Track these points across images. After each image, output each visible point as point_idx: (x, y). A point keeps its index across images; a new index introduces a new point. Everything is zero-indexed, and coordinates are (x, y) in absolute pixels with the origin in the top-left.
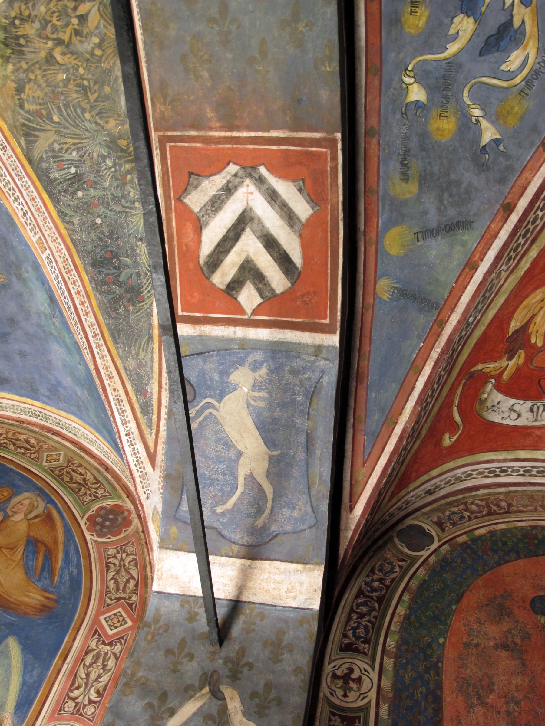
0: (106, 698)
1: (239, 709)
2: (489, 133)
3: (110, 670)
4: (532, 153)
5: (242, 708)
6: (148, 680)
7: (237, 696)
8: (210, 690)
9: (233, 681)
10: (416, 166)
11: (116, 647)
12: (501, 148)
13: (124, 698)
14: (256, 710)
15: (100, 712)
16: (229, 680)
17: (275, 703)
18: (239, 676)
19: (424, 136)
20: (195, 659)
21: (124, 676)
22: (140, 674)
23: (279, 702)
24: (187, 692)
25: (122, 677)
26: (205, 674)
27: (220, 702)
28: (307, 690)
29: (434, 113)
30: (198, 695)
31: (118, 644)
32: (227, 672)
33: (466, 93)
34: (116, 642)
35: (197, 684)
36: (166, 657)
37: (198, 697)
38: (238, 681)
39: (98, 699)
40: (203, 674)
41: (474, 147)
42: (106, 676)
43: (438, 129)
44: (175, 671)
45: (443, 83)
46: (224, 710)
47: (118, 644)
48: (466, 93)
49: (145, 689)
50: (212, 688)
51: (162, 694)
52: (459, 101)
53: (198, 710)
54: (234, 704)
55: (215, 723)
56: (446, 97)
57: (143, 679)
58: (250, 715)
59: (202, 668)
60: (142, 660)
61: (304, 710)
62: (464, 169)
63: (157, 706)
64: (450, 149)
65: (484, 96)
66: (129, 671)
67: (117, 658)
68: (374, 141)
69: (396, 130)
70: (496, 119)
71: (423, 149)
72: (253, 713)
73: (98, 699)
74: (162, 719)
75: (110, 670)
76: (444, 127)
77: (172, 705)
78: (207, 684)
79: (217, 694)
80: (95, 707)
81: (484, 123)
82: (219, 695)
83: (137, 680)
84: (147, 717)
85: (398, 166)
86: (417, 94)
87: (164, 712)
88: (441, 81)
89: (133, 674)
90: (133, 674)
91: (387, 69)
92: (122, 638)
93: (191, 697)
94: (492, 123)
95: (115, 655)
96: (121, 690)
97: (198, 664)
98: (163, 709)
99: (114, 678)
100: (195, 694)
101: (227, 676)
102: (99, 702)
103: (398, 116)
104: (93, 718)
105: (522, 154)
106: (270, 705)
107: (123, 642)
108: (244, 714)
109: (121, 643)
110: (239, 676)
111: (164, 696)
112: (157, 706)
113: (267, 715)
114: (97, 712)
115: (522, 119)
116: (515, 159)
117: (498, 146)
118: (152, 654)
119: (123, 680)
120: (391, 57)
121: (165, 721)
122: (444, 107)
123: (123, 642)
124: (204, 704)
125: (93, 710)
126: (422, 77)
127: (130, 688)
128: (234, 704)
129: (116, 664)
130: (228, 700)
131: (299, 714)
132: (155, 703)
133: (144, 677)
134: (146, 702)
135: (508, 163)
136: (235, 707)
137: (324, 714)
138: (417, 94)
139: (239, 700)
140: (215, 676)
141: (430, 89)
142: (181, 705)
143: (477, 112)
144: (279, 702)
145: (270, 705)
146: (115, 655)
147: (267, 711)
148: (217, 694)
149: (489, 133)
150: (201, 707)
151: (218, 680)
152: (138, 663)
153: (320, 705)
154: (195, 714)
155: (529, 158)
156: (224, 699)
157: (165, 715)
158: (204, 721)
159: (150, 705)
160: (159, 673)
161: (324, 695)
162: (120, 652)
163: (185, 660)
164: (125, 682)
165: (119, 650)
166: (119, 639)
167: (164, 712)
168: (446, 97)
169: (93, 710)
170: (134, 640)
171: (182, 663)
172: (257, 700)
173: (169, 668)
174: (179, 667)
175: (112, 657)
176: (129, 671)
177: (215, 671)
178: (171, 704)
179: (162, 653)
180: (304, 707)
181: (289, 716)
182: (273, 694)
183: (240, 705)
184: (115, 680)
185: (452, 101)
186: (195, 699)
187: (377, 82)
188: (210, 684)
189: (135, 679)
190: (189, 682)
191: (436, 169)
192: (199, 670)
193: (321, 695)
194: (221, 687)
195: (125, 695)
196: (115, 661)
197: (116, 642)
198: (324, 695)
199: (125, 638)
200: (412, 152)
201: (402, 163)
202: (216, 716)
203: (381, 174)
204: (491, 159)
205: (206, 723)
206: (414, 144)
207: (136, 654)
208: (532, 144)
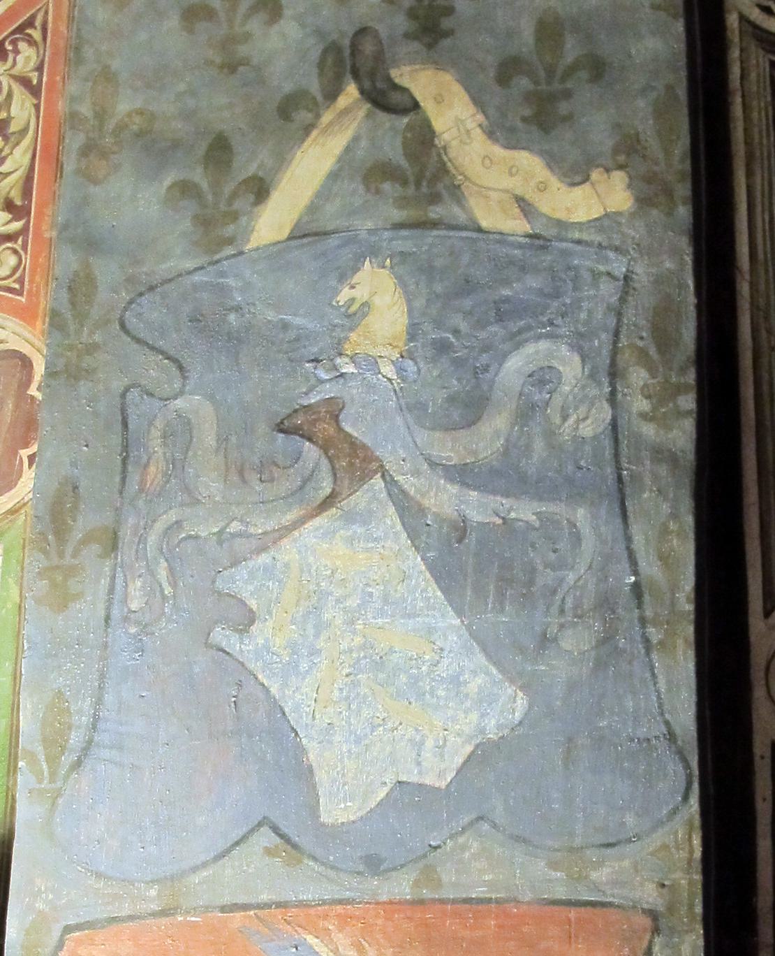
0: (40, 214)
1: (471, 124)
3: (24, 131)
5: (480, 117)
6: (153, 117)
7: (457, 88)
8: (362, 92)
9: (430, 46)
11: (19, 58)
13: (93, 190)
14: (527, 112)
15: (35, 257)
16: (415, 46)
17: (584, 75)
18: (446, 23)
20: (288, 12)
21: (72, 127)
22: (123, 106)
23: (597, 68)
24: (292, 115)
25: (68, 134)
26: (332, 49)
27: (406, 120)
28: (681, 10)
30: (327, 117)
31: (22, 46)
32: (401, 23)
34: (14, 42)
35: (314, 87)
36: (191, 31)
37: (331, 124)
38: (446, 42)
39: (17, 225)
40: (325, 51)
42: (18, 152)
44: (231, 67)
46: (423, 140)
47: (22, 46)
49: (153, 147)
50: (367, 84)
51: (211, 148)
53: (340, 160)
54: (452, 112)
55: (405, 183)
57: (137, 119)
58: (512, 130)
59: (319, 33)
60: (115, 64)
61: (683, 74)
63: (204, 185)
66: (85, 109)
67: (35, 91)
72: (520, 124)
73: (17, 225)
74: (234, 217)
75: (24, 131)
77: (252, 169)
78: (349, 76)
79: (386, 98)
80: (15, 252)
82: (395, 98)
83: (121, 128)
84: (187, 225)
87: (234, 195)
89: (101, 115)
90: (101, 115)
92: (30, 23)
93: (308, 129)
95: (25, 82)
96: (78, 171)
97: (303, 26)
98: (228, 189)
99: (46, 148)
100: (318, 116)
101: (407, 36)
102: (24, 231)
104: (21, 281)
106: (569, 85)
107: (36, 34)
108: (491, 134)
109: (31, 42)
110: (446, 23)
111: (219, 151)
112: (204, 185)
113: (568, 118)
114: (27, 261)
118: (143, 36)
119: (74, 142)
121: (244, 220)
123: (36, 34)
124: (356, 139)
125: (13, 261)
127: (104, 155)
128: (452, 112)
129: (37, 107)
130: (428, 105)
131: (669, 88)
132: (198, 176)
133: (140, 112)
134: (168, 182)
136: (459, 122)
137: (753, 75)
139: (466, 98)
140: (368, 47)
142: (282, 160)
144: (597, 68)
145: (569, 85)
146: (25, 82)
147: (564, 107)
148: (386, 98)
150: (348, 149)
151: (379, 57)
152: (107, 76)
153: (735, 53)
154: (334, 176)
156: (416, 106)
157: (238, 205)
158: (368, 190)
159: (185, 189)
160: (182, 87)
161: (743, 19)
162: (39, 68)
163: (255, 25)
164: (84, 146)
165: (32, 64)
166: (20, 29)
167: (234, 195)
169: (13, 261)
170: (71, 19)
171: (247, 37)
172: (523, 83)
173: (209, 63)
174: (243, 50)
175: (18, 90)
176: (85, 109)
177: (362, 31)
178: (246, 165)
179: (173, 21)
180: (683, 62)
181: (641, 103)
182: (572, 50)
183: (472, 109)
184: (50, 155)
186: (324, 131)
188: (356, 75)
189: (111, 125)
190: (288, 87)
192: (312, 41)
193: (732, 20)
194: (394, 73)
195: (96, 182)
196: (30, 101)
197: (14, 42)
198: (743, 19)
199: (38, 23)
202: (404, 163)
205: (378, 192)
207: (88, 52)
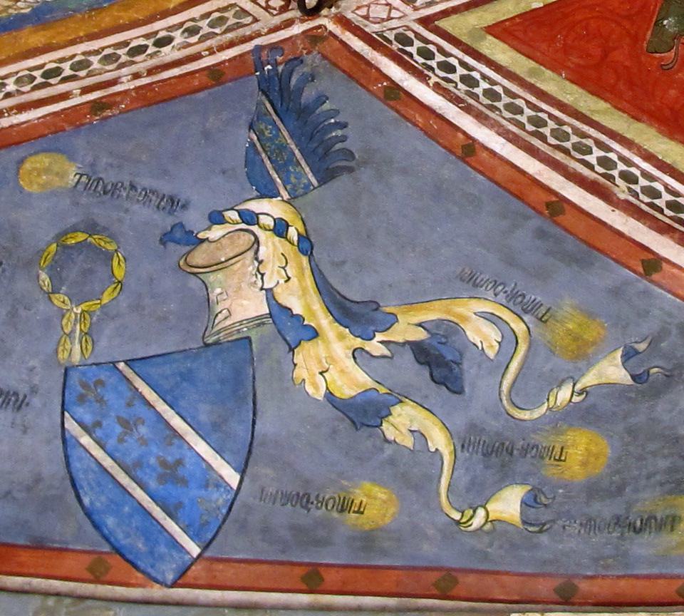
2: (612, 370)
4: (660, 291)
10: (649, 501)
12: (642, 347)
19: (593, 490)
29: (550, 471)
33: (525, 415)
41: (633, 395)
43: (584, 464)
45: (496, 454)
48: (525, 415)
52: (536, 425)
56: (525, 451)
62: (670, 411)
64: (627, 439)
65: (535, 382)
68: (584, 586)
69: (572, 544)
70: (583, 355)
71: (620, 490)
76: (583, 453)
81: (589, 380)
85: (645, 537)
86: (508, 504)
88: (494, 459)
91: (450, 559)
94: (590, 365)
103: (544, 538)
105: (662, 309)
115: (591, 315)
116: (669, 320)
117: (637, 353)
120: (430, 551)
122: (538, 453)
126: (478, 493)
135: (674, 331)
138: (508, 504)
141: (505, 478)
143: (564, 394)
149: (612, 370)
155: (670, 296)
168: (525, 451)
185: (535, 438)
187: (471, 579)
191: (663, 464)
200: (620, 510)
201: (638, 531)
203: (655, 571)
204: (660, 363)
206: (605, 509)
208: (646, 293)
